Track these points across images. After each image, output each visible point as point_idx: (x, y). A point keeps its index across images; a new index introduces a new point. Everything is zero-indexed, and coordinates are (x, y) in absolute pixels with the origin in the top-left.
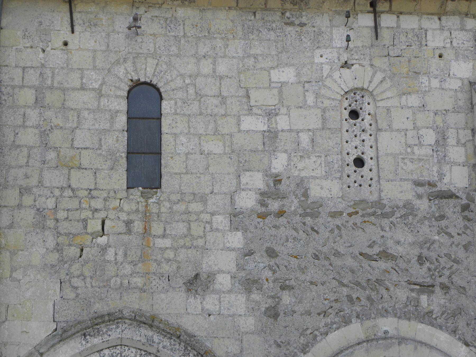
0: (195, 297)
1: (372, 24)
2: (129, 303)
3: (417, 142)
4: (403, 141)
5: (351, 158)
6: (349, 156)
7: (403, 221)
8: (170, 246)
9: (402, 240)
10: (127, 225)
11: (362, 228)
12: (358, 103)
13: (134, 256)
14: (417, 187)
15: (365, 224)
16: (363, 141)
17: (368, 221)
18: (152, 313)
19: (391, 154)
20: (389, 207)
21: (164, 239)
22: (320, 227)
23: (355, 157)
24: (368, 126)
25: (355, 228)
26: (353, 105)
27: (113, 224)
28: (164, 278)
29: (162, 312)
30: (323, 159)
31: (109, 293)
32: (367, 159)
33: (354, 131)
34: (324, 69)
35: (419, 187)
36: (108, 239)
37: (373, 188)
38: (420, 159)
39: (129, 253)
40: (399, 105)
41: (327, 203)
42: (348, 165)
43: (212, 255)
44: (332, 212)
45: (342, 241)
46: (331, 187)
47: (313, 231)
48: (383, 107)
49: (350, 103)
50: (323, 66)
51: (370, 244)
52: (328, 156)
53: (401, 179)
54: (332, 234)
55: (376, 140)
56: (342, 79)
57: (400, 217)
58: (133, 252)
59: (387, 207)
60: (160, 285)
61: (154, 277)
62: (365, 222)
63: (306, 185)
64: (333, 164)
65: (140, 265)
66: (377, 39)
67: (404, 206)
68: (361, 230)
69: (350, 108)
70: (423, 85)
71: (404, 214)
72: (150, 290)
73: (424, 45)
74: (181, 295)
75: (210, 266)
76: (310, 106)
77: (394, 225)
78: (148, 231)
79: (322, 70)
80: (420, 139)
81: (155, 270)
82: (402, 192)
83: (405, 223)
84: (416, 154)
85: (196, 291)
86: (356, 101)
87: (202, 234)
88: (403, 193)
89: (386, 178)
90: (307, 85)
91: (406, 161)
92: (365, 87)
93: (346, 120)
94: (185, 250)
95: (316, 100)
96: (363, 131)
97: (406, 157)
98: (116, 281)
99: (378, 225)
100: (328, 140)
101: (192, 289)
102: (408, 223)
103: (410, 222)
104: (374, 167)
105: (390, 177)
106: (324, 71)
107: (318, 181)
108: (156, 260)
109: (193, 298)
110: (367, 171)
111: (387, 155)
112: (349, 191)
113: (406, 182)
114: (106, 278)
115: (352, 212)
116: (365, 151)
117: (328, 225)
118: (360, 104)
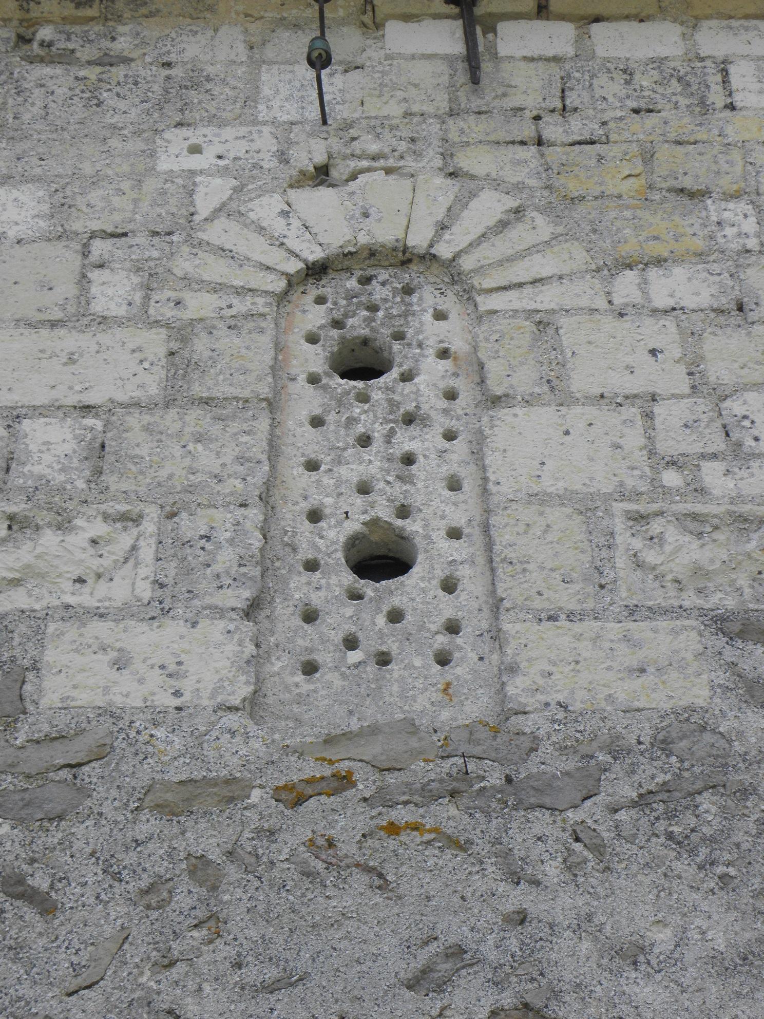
1: (458, 47)
3: (718, 444)
4: (634, 439)
5: (331, 534)
6: (323, 524)
7: (661, 826)
9: (663, 938)
11: (369, 870)
12: (380, 314)
14: (739, 644)
15: (392, 844)
16: (409, 460)
17: (416, 827)
19: (564, 498)
20: (562, 749)
22: (72, 876)
23: (353, 526)
24: (432, 402)
25: (320, 866)
26: (350, 322)
30: (149, 527)
32: (427, 537)
33: (352, 421)
34: (200, 192)
35: (750, 646)
37: (458, 671)
38: (743, 519)
40: (601, 303)
41: (144, 737)
42: (312, 566)
44: (167, 786)
45: (225, 951)
46: (183, 657)
47: (20, 896)
48: (516, 311)
49: (336, 315)
50: (198, 179)
51: (426, 971)
52: (184, 515)
53: (632, 611)
54: (154, 914)
55: (478, 454)
56: (295, 223)
57: (634, 804)
59: (547, 748)
62: (393, 829)
63: (17, 652)
64: (209, 547)
66: (475, 80)
67: (664, 745)
68: (359, 881)
69: (335, 333)
70: (729, 231)
71: (665, 787)
73: (720, 104)
76: (104, 318)
77: (598, 849)
79: (191, 194)
80: (735, 435)
82: (643, 671)
83: (670, 836)
84: (716, 492)
86: (373, 308)
88: (649, 679)
89: (537, 604)
90: (99, 248)
91: (656, 527)
92: (418, 240)
93: (313, 380)
95: (147, 298)
96: (409, 420)
97: (655, 507)
99: (481, 847)
100: (191, 447)
102: (695, 837)
103: (707, 830)
104: (464, 572)
105: (566, 599)
106: (198, 198)
107: (99, 629)
110: (424, 591)
111: (539, 499)
112: (305, 687)
113: (663, 624)
115: (310, 781)
116: (417, 500)
117: (130, 858)
118: (390, 316)
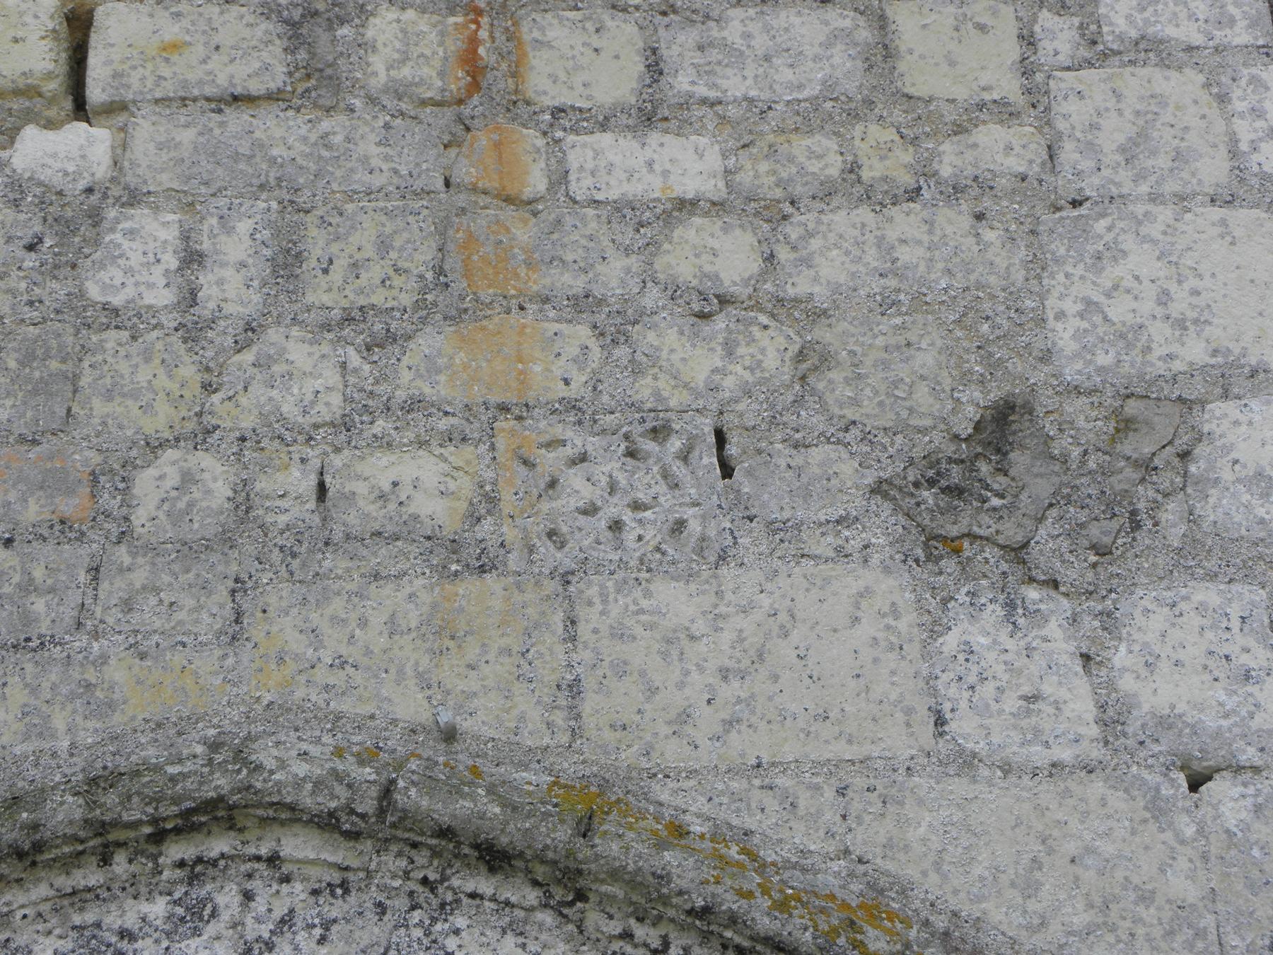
0: (1010, 606)
2: (321, 675)
8: (712, 187)
10: (296, 36)
13: (375, 272)
18: (569, 767)
21: (654, 137)
27: (172, 31)
28: (675, 444)
29: (672, 753)
31: (113, 589)
36: (123, 144)
39: (316, 243)
43: (1128, 242)
58: (364, 238)
60: (637, 506)
61: (578, 440)
65: (428, 342)
72: (545, 548)
74: (866, 593)
75: (1129, 336)
78: (498, 81)
81: (579, 379)
85: (1017, 552)
87: (1009, 87)
94: (864, 214)
98: (188, 479)
101: (973, 537)
108: (583, 303)
109: (995, 612)
114: (84, 458)
